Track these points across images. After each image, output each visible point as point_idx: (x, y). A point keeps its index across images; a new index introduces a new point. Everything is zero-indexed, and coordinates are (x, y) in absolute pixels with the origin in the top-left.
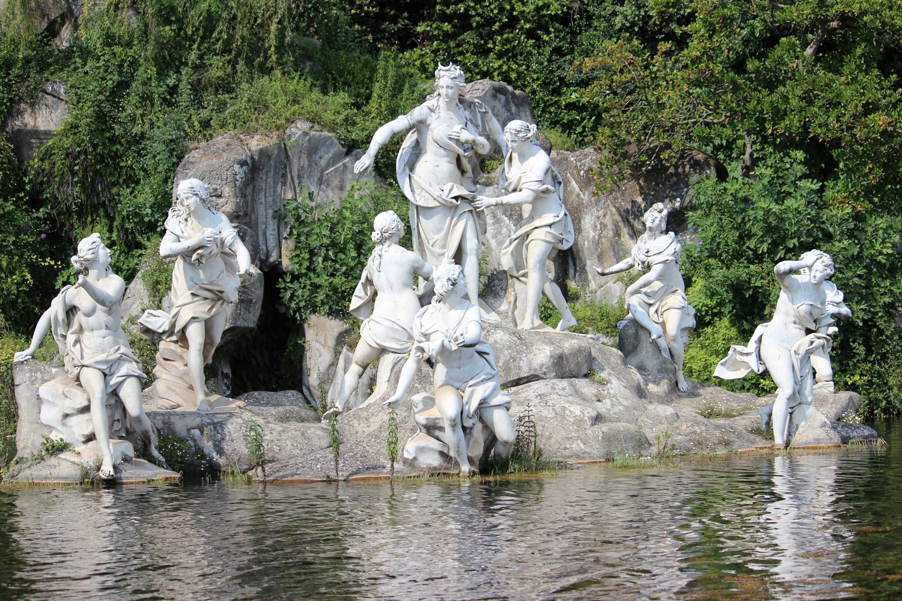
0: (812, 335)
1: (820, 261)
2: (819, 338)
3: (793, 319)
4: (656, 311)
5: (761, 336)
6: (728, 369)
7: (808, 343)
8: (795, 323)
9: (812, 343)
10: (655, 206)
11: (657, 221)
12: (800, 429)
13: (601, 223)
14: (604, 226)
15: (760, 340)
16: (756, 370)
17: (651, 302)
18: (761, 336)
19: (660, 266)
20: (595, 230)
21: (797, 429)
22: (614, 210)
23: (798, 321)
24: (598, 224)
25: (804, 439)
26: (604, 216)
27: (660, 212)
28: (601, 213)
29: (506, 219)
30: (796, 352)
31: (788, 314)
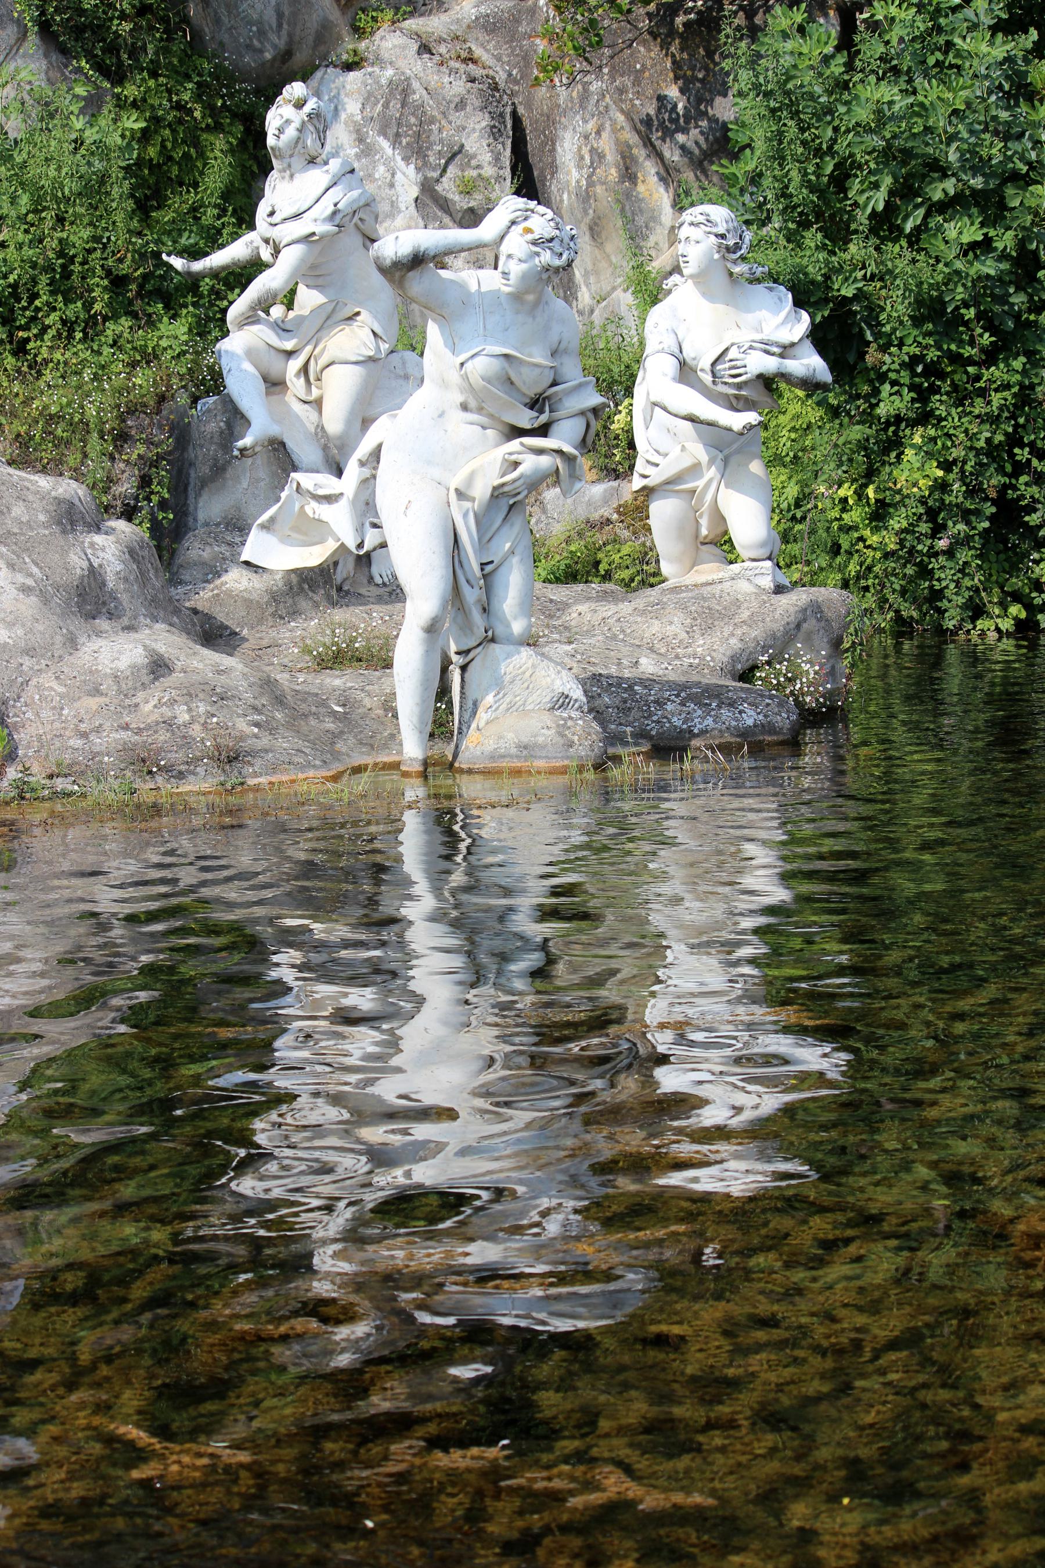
0: (515, 444)
1: (517, 229)
2: (540, 452)
3: (460, 398)
4: (305, 369)
5: (380, 447)
6: (285, 540)
7: (497, 467)
8: (465, 407)
9: (516, 464)
10: (287, 91)
11: (291, 132)
12: (482, 716)
13: (593, 151)
14: (598, 156)
15: (376, 454)
16: (352, 545)
17: (289, 345)
18: (380, 447)
19: (297, 250)
20: (580, 167)
21: (474, 713)
22: (621, 118)
23: (473, 404)
24: (585, 151)
25: (490, 745)
26: (598, 133)
27: (299, 105)
28: (591, 125)
29: (385, 144)
30: (460, 494)
31: (444, 384)
